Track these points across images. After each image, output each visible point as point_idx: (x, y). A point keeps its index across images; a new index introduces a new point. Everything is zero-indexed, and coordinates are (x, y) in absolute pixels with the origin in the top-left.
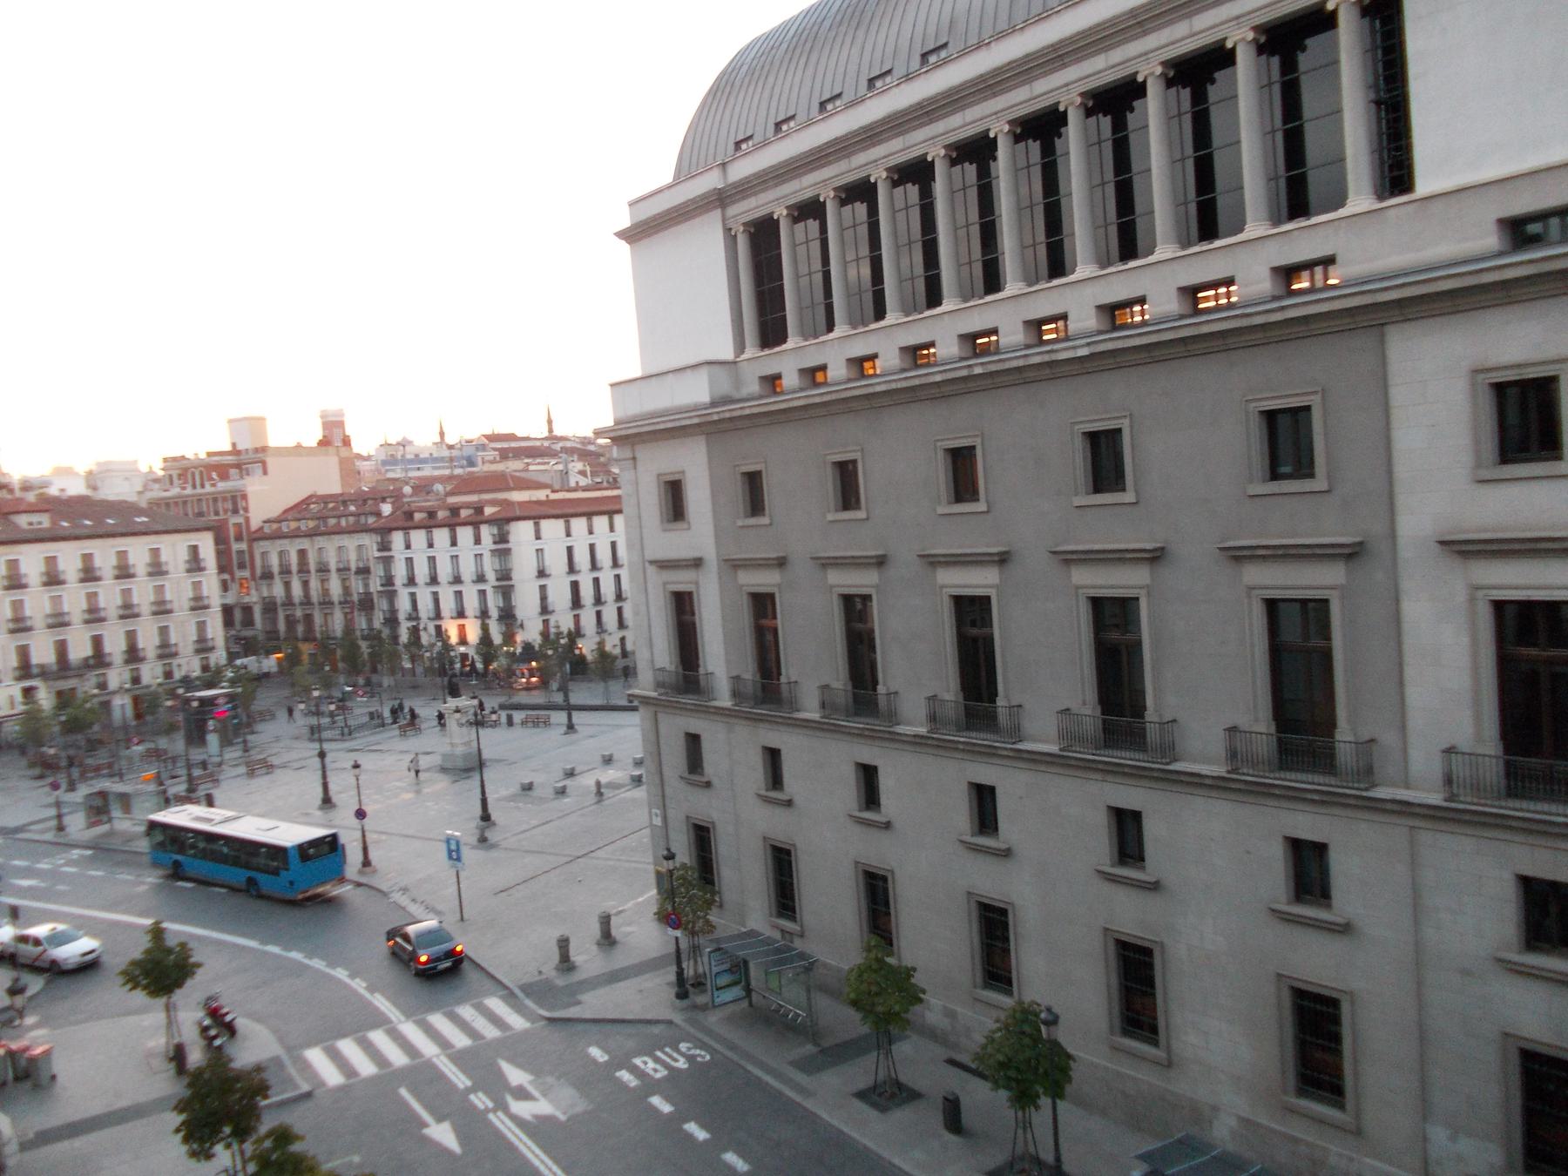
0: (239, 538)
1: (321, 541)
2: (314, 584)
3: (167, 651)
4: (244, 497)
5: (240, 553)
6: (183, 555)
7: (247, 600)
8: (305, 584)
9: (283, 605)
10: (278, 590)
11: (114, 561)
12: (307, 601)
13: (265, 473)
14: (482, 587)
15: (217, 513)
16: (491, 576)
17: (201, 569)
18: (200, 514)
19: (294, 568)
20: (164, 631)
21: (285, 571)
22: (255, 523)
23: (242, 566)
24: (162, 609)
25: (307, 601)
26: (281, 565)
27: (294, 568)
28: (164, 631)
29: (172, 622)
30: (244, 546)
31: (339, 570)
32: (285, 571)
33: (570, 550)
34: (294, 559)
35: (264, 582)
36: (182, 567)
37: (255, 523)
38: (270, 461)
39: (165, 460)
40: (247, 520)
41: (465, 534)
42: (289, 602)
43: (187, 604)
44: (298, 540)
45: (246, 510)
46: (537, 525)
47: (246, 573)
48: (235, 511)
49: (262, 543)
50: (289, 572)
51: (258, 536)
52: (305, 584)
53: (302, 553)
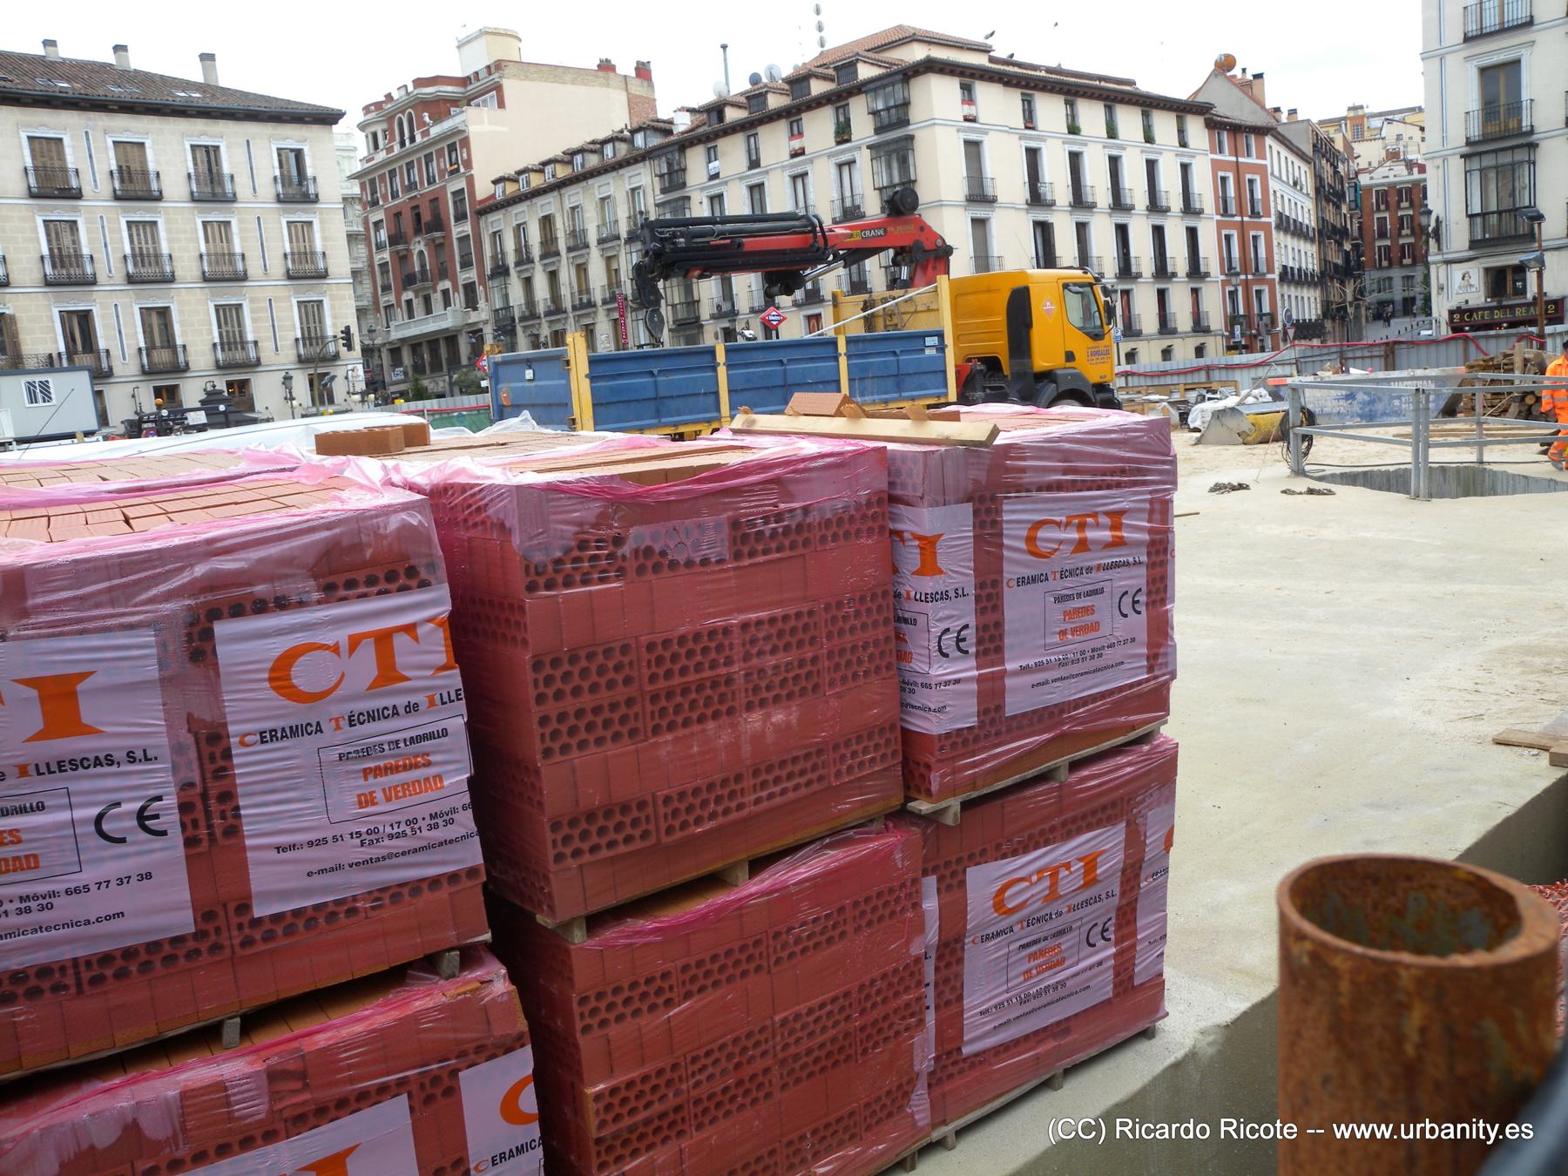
0: (461, 217)
1: (573, 196)
2: (566, 275)
3: (239, 356)
4: (465, 142)
5: (463, 240)
6: (268, 167)
7: (474, 317)
9: (523, 319)
11: (109, 160)
12: (556, 309)
13: (501, 104)
17: (309, 199)
19: (536, 252)
20: (229, 315)
21: (524, 259)
23: (466, 264)
24: (224, 272)
25: (556, 309)
26: (518, 251)
27: (536, 252)
28: (229, 315)
30: (467, 228)
31: (601, 241)
32: (524, 259)
33: (1033, 155)
34: (534, 235)
35: (496, 283)
36: (267, 190)
37: (483, 189)
39: (367, 109)
40: (470, 180)
42: (531, 314)
43: (277, 267)
44: (540, 201)
45: (468, 164)
47: (472, 275)
49: (492, 217)
51: (492, 207)
52: (553, 276)
53: (547, 221)
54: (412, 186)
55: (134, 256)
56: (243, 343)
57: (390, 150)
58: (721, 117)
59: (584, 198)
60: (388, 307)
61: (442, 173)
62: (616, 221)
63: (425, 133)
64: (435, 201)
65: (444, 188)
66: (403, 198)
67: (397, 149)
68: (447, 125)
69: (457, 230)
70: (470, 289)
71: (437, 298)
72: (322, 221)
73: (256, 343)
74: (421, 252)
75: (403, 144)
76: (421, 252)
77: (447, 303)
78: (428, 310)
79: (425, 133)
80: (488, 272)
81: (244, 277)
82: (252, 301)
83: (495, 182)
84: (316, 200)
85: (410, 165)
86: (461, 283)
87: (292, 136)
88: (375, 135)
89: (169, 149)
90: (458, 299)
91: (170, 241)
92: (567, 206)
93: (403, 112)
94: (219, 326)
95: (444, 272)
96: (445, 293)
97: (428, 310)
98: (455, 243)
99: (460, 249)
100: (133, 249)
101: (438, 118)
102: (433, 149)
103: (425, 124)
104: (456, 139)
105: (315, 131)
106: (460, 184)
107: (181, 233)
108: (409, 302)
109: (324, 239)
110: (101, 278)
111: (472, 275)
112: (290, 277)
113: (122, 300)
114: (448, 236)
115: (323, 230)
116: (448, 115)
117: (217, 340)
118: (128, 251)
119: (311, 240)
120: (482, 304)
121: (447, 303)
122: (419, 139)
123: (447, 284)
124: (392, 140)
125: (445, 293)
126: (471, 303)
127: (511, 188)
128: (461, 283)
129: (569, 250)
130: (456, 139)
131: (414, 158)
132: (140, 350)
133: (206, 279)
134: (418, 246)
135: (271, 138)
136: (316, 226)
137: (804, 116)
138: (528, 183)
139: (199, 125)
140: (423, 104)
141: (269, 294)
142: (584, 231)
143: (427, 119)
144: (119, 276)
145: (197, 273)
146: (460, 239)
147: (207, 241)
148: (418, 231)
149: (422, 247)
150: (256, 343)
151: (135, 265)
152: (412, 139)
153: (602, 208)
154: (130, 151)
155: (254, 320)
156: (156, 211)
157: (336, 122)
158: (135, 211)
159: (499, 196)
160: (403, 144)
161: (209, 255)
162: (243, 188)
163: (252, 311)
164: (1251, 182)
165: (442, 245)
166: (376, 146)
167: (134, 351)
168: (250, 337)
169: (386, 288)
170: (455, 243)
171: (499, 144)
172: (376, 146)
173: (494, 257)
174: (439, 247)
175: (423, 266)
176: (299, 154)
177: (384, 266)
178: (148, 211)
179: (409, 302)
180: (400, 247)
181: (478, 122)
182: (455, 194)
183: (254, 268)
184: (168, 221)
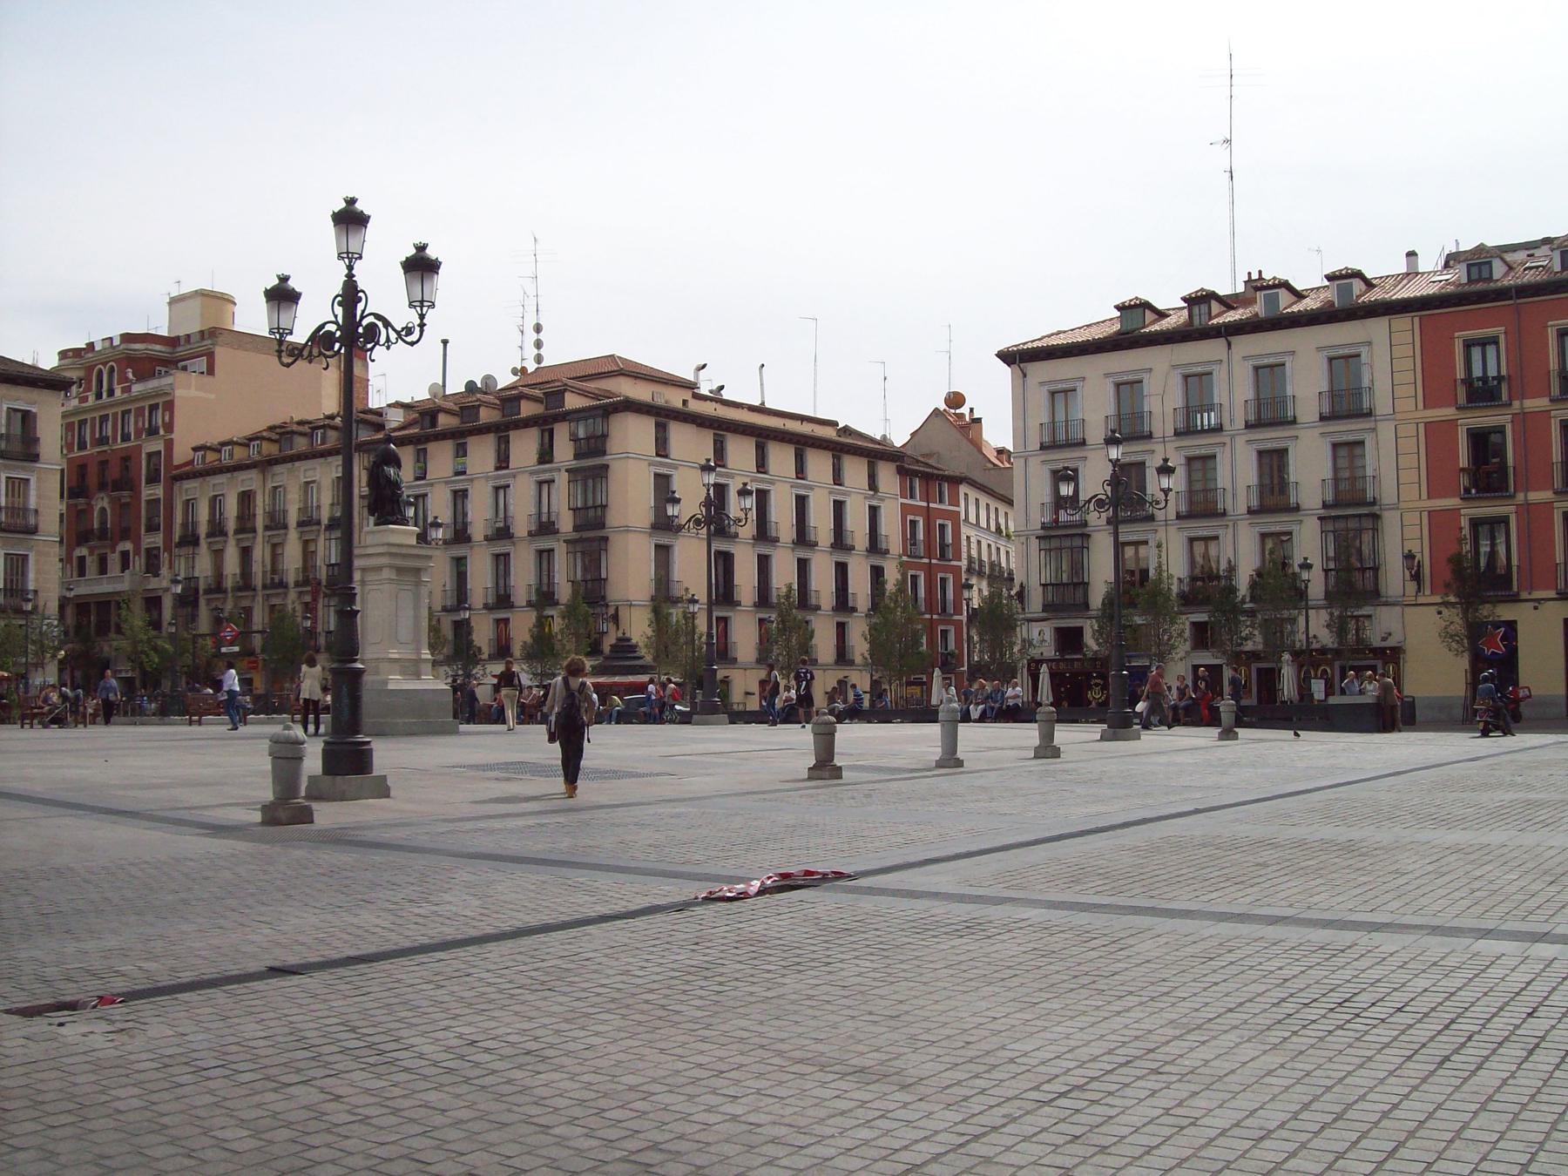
0: (153, 479)
2: (260, 553)
4: (170, 406)
5: (153, 503)
7: (154, 583)
8: (246, 553)
9: (208, 591)
10: (203, 567)
13: (211, 371)
14: (545, 543)
15: (126, 438)
16: (566, 523)
18: (103, 440)
19: (231, 525)
21: (217, 529)
22: (181, 453)
23: (152, 528)
25: (245, 583)
26: (211, 521)
27: (231, 525)
30: (159, 491)
31: (300, 524)
32: (217, 529)
34: (231, 508)
35: (184, 551)
37: (181, 453)
38: (221, 353)
40: (169, 445)
41: (524, 447)
42: (217, 587)
44: (242, 475)
45: (169, 427)
46: (661, 430)
47: (157, 539)
48: (153, 431)
49: (189, 485)
50: (224, 533)
52: (246, 553)
53: (246, 498)
54: (103, 440)
58: (434, 423)
59: (292, 479)
61: (138, 433)
62: (319, 507)
63: (125, 390)
64: (127, 459)
68: (153, 384)
69: (147, 492)
71: (114, 560)
74: (103, 510)
75: (99, 396)
78: (103, 570)
79: (127, 390)
80: (176, 538)
83: (195, 449)
85: (104, 419)
86: (144, 546)
90: (138, 563)
92: (270, 485)
93: (104, 364)
95: (125, 534)
96: (125, 556)
97: (103, 570)
98: (143, 505)
99: (147, 511)
101: (141, 377)
102: (132, 407)
103: (127, 379)
104: (160, 400)
106: (157, 445)
111: (157, 539)
116: (152, 375)
120: (164, 571)
122: (118, 393)
123: (127, 546)
125: (125, 556)
126: (152, 567)
127: (211, 457)
128: (144, 546)
129: (267, 528)
130: (160, 400)
131: (110, 412)
134: (102, 502)
137: (512, 434)
138: (231, 455)
140: (130, 360)
142: (285, 512)
143: (130, 376)
146: (148, 502)
148: (102, 486)
149: (105, 503)
152: (111, 392)
153: (306, 492)
159: (198, 466)
160: (99, 396)
164: (942, 527)
165: (128, 504)
170: (143, 505)
171: (205, 412)
173: (185, 525)
174: (122, 508)
175: (103, 522)
181: (186, 388)
182: (150, 455)
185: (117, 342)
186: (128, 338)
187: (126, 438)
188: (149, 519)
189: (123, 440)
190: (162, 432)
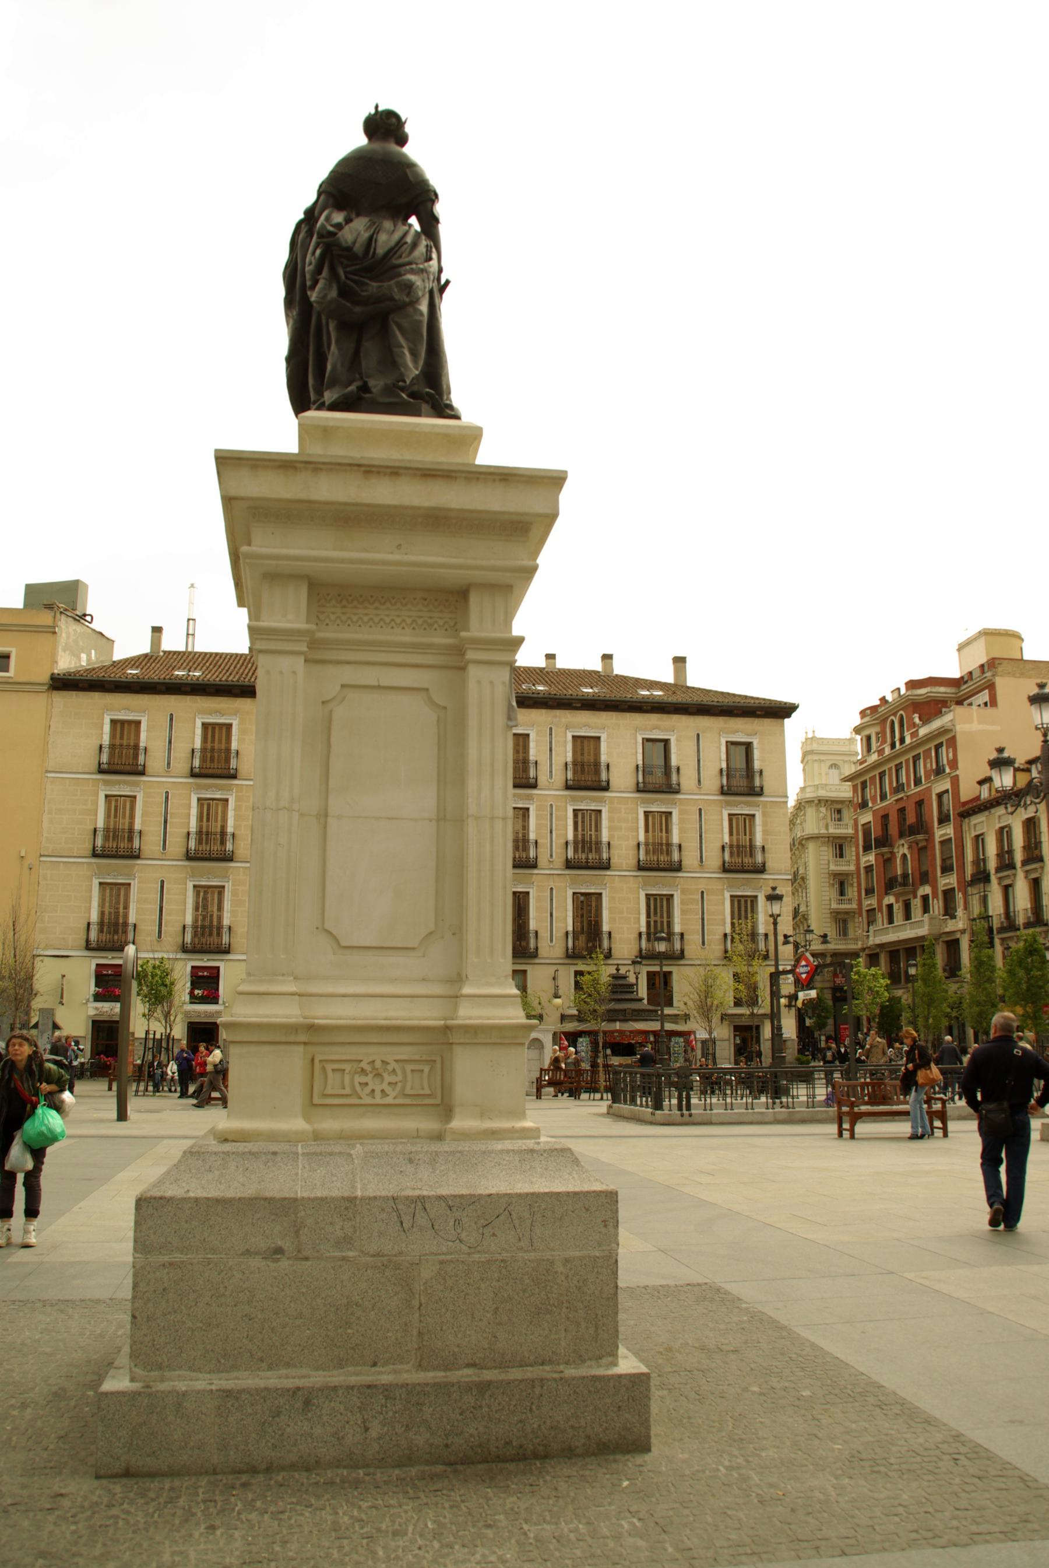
0: (943, 819)
4: (952, 742)
5: (945, 843)
6: (715, 758)
7: (951, 926)
11: (566, 753)
15: (918, 782)
20: (659, 907)
23: (946, 869)
24: (659, 860)
28: (659, 907)
29: (682, 893)
30: (949, 831)
36: (712, 781)
39: (863, 713)
43: (713, 858)
45: (954, 764)
47: (951, 880)
48: (939, 771)
54: (899, 788)
55: (576, 842)
56: (670, 935)
57: (881, 752)
60: (871, 912)
61: (927, 777)
63: (914, 735)
65: (929, 789)
66: (891, 799)
67: (887, 751)
68: (936, 724)
69: (941, 833)
70: (949, 895)
71: (917, 904)
72: (764, 815)
73: (682, 935)
74: (904, 856)
75: (893, 746)
76: (904, 856)
77: (926, 909)
78: (908, 916)
81: (678, 868)
82: (683, 892)
84: (760, 793)
86: (941, 888)
87: (741, 729)
88: (869, 738)
89: (622, 744)
90: (937, 906)
91: (611, 829)
93: (895, 714)
94: (648, 916)
95: (925, 878)
96: (925, 898)
97: (908, 916)
98: (937, 846)
99: (942, 852)
100: (575, 836)
101: (926, 720)
102: (921, 750)
103: (914, 725)
105: (767, 724)
106: (945, 785)
107: (623, 824)
108: (890, 907)
109: (765, 832)
110: (543, 861)
111: (951, 880)
112: (725, 870)
113: (557, 884)
114: (930, 839)
115: (765, 824)
116: (939, 713)
117: (644, 929)
118: (570, 836)
119: (752, 833)
121: (926, 909)
123: (926, 890)
124: (884, 742)
125: (925, 898)
126: (949, 911)
130: (943, 739)
131: (903, 759)
132: (567, 933)
133: (640, 868)
134: (902, 849)
135: (721, 731)
136: (758, 820)
139: (654, 719)
141: (702, 887)
143: (917, 720)
144: (559, 860)
145: (633, 862)
146: (942, 842)
147: (647, 831)
148: (901, 835)
149: (906, 851)
150: (682, 935)
151: (576, 851)
152: (902, 740)
154: (586, 747)
155: (683, 912)
156: (602, 800)
157: (789, 716)
158: (582, 799)
160: (893, 746)
161: (647, 844)
162: (687, 780)
163: (682, 903)
165: (925, 847)
166: (869, 749)
167: (562, 934)
168: (677, 929)
169: (869, 892)
170: (937, 846)
172: (869, 749)
174: (923, 851)
176: (748, 746)
177: (869, 869)
178: (594, 800)
179: (890, 907)
180: (885, 850)
182: (940, 796)
183: (690, 859)
184: (611, 811)
185: (903, 691)
186: (912, 684)
187: (918, 782)
188: (943, 860)
189: (915, 785)
190: (948, 770)
